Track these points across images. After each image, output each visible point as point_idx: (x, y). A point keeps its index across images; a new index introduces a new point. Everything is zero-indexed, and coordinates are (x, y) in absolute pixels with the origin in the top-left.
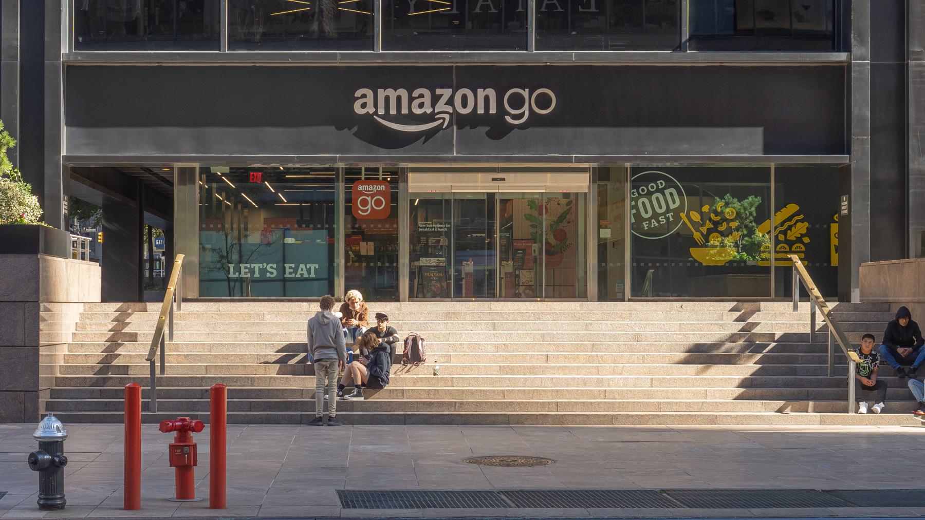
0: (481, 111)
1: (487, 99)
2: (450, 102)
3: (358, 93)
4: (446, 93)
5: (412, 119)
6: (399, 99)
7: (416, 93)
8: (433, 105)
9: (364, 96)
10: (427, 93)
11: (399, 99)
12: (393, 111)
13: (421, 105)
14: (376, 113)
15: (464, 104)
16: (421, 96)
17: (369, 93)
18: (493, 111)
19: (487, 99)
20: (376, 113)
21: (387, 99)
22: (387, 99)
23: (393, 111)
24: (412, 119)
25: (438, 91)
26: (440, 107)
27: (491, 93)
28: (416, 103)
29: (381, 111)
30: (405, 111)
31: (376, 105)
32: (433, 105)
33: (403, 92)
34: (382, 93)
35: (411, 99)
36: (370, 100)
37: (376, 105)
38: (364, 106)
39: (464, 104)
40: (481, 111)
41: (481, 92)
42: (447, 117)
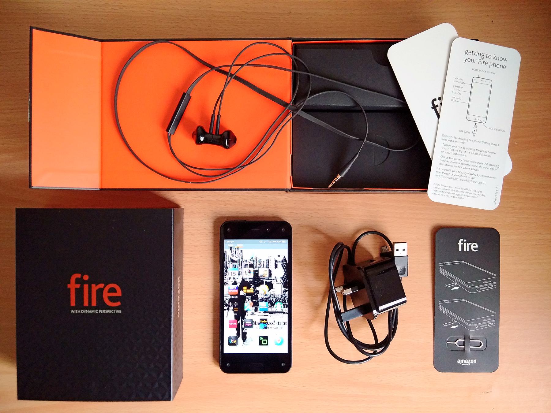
0: (474, 363)
2: (470, 361)
3: (458, 360)
4: (470, 360)
8: (468, 361)
12: (463, 362)
15: (472, 362)
23: (463, 362)
24: (465, 364)
26: (469, 362)
27: (476, 360)
28: (466, 362)
29: (461, 362)
30: (464, 363)
32: (468, 361)
33: (464, 360)
34: (461, 360)
35: (465, 361)
39: (472, 362)
40: (474, 363)
41: (474, 360)
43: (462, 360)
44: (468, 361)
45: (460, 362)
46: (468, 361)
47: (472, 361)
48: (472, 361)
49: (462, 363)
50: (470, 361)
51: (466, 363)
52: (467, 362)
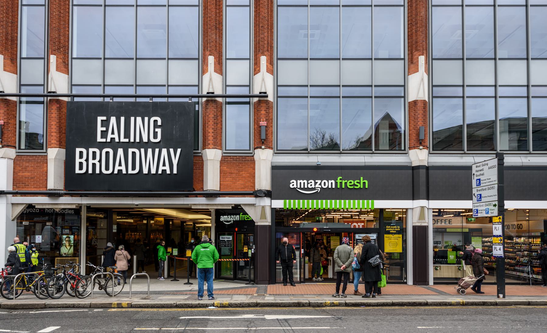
0: (330, 187)
1: (332, 183)
2: (320, 184)
3: (291, 182)
4: (319, 181)
5: (308, 189)
6: (304, 183)
7: (309, 182)
9: (293, 182)
10: (313, 181)
11: (304, 183)
12: (302, 187)
13: (311, 185)
14: (297, 187)
16: (311, 182)
17: (295, 181)
18: (334, 187)
19: (332, 183)
20: (297, 187)
21: (300, 183)
22: (300, 183)
23: (302, 187)
24: (308, 189)
25: (316, 181)
26: (317, 186)
27: (333, 182)
28: (309, 185)
29: (299, 187)
30: (306, 187)
31: (297, 185)
32: (315, 185)
33: (306, 181)
34: (299, 182)
35: (308, 183)
36: (295, 183)
37: (297, 185)
38: (293, 185)
40: (330, 187)
41: (330, 182)
42: (319, 189)
43: (301, 181)
44: (316, 183)
45: (295, 186)
46: (316, 183)
47: (325, 183)
48: (325, 183)
49: (300, 188)
50: (320, 184)
51: (310, 187)
52: (313, 186)
